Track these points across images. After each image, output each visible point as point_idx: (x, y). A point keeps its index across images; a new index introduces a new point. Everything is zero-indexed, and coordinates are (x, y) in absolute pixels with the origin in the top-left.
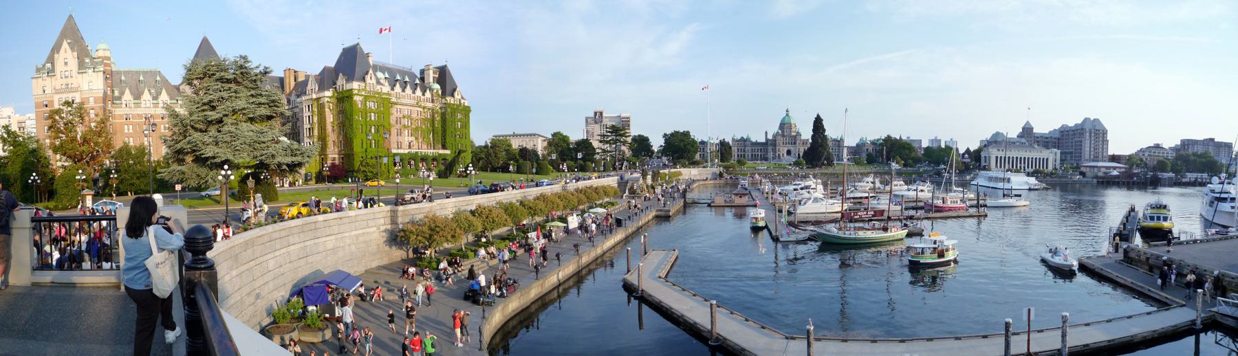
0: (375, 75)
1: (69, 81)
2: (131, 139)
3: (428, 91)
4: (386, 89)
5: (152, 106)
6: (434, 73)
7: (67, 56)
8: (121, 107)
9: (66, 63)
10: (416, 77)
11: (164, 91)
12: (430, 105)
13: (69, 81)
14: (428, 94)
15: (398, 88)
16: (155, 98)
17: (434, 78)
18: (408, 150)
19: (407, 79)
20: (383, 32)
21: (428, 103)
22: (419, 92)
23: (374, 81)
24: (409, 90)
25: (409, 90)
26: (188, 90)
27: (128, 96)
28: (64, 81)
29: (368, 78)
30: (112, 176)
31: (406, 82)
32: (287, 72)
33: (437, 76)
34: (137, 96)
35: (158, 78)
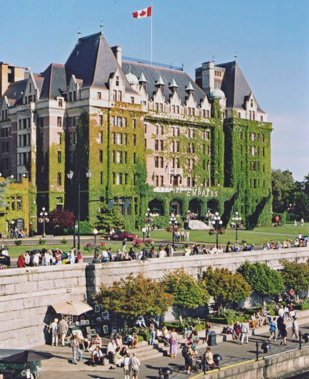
0: (125, 79)
3: (206, 100)
4: (141, 96)
6: (217, 73)
10: (189, 79)
15: (159, 98)
17: (216, 80)
18: (171, 189)
19: (174, 84)
20: (146, 10)
21: (206, 120)
22: (191, 103)
23: (121, 87)
24: (176, 100)
25: (176, 100)
29: (113, 82)
31: (172, 89)
33: (221, 78)
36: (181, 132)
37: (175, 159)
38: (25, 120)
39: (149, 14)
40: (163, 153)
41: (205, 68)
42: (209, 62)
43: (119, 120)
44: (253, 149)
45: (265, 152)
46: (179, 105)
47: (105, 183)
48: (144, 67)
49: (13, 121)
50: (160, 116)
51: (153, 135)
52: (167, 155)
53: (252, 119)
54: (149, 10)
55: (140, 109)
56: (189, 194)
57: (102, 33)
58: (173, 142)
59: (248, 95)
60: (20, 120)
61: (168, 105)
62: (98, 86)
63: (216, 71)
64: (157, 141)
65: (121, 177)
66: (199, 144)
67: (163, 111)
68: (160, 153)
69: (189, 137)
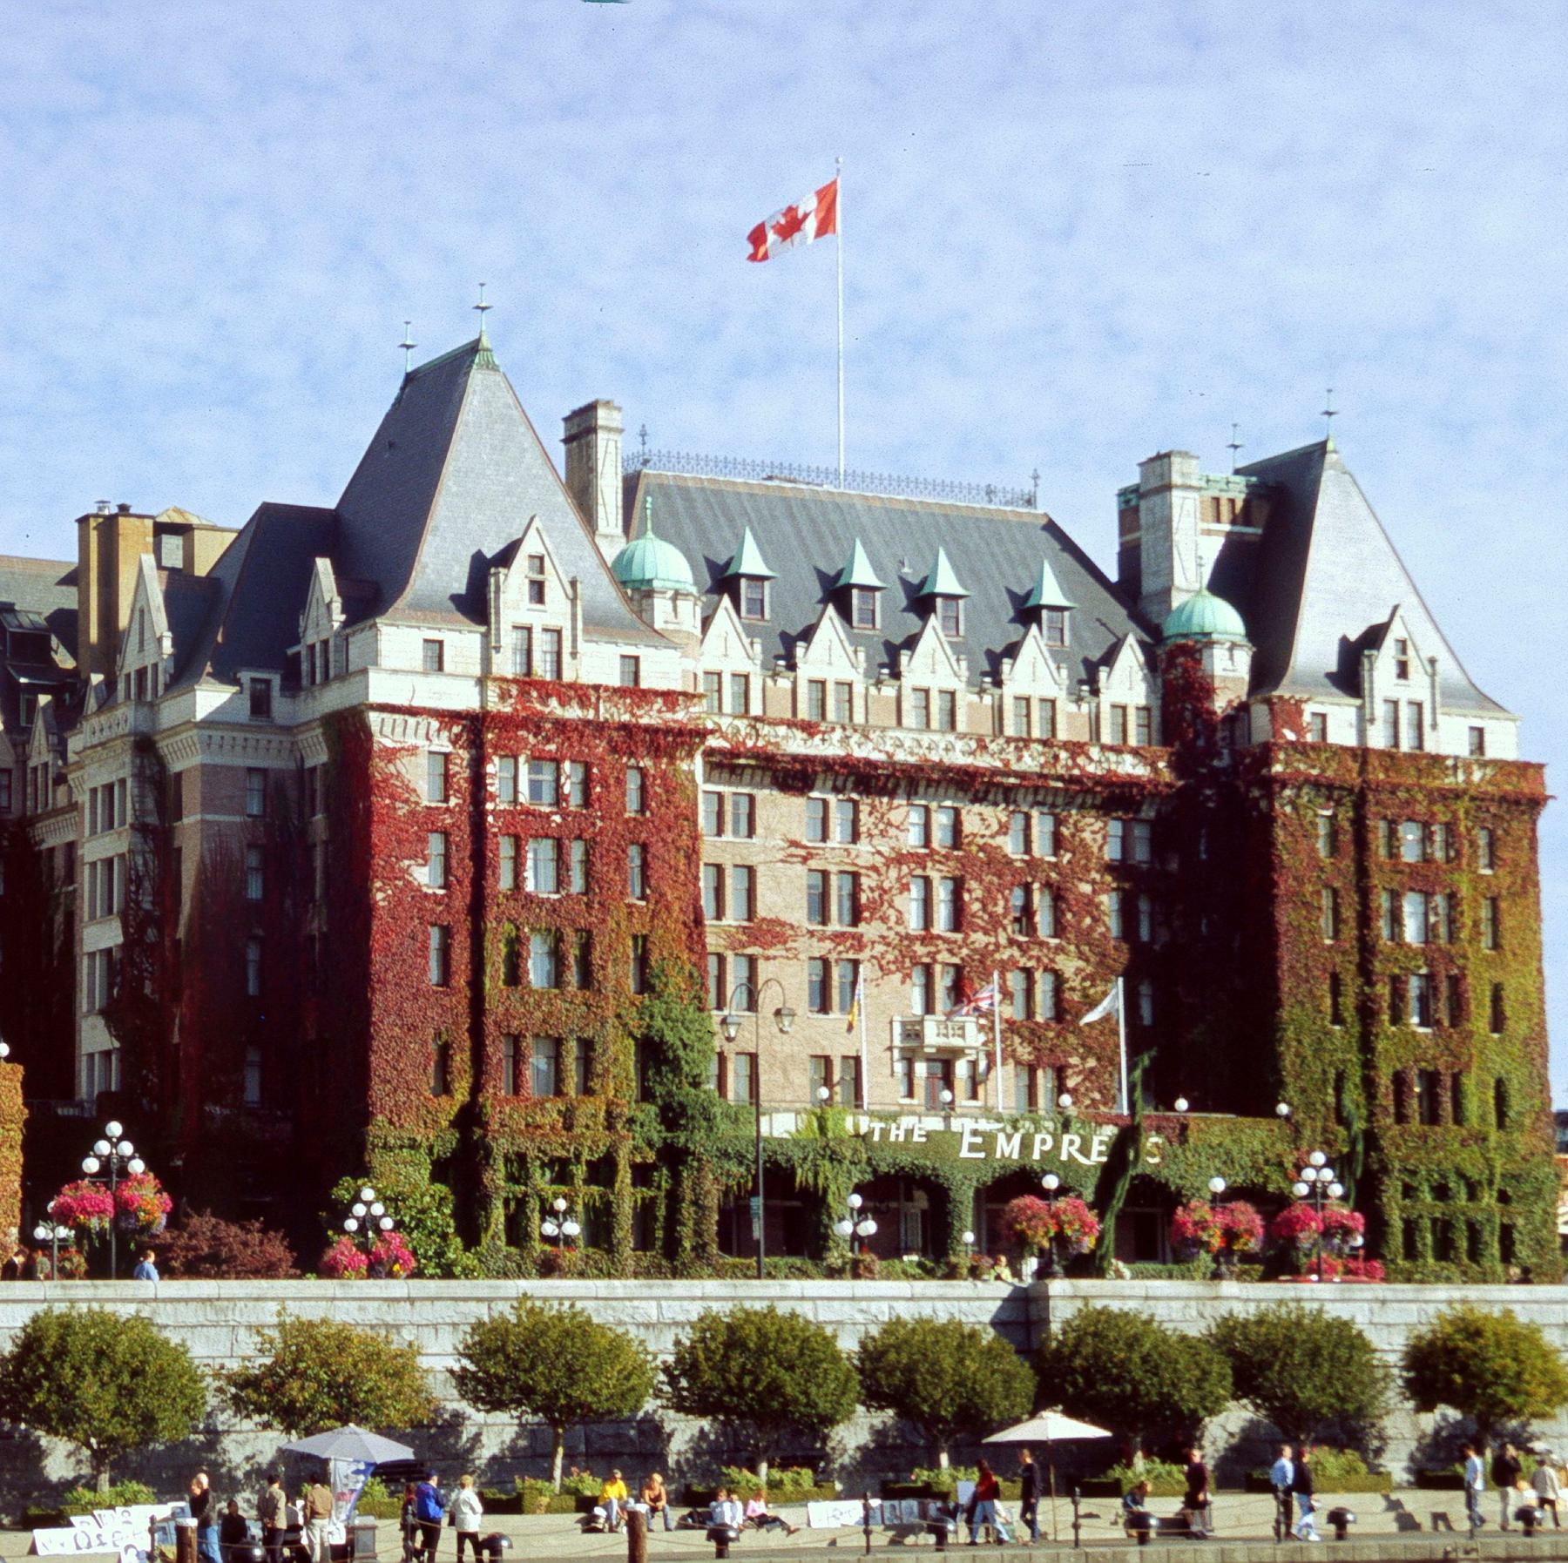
3: (1131, 657)
36: (971, 824)
37: (938, 968)
38: (109, 788)
39: (825, 225)
40: (859, 938)
41: (1154, 483)
42: (1168, 455)
43: (547, 776)
44: (1411, 907)
45: (1508, 922)
46: (959, 685)
47: (461, 1093)
48: (784, 499)
50: (829, 747)
51: (795, 844)
52: (880, 948)
53: (1406, 745)
54: (827, 197)
55: (669, 716)
56: (973, 1147)
57: (485, 342)
58: (927, 882)
59: (1383, 619)
60: (94, 791)
61: (889, 691)
62: (424, 610)
63: (1217, 500)
64: (825, 875)
65: (557, 1059)
66: (1086, 888)
67: (859, 718)
68: (838, 938)
69: (1028, 848)
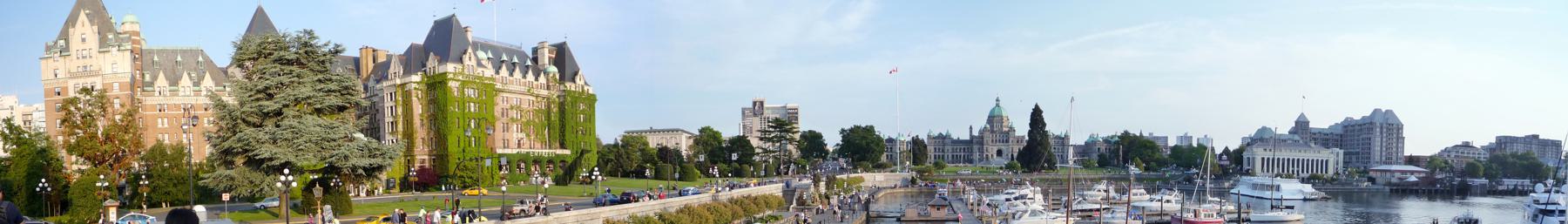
0: (475, 55)
1: (87, 62)
2: (166, 136)
3: (542, 75)
4: (489, 72)
5: (192, 94)
6: (550, 52)
7: (85, 30)
8: (153, 95)
9: (84, 40)
10: (528, 57)
11: (208, 76)
12: (545, 92)
13: (87, 62)
14: (542, 79)
15: (504, 72)
16: (197, 84)
17: (550, 58)
18: (518, 150)
19: (515, 60)
21: (542, 91)
22: (530, 77)
23: (474, 62)
24: (518, 74)
25: (518, 74)
26: (238, 74)
27: (162, 81)
28: (81, 62)
29: (466, 58)
30: (141, 183)
31: (514, 64)
32: (364, 51)
33: (554, 56)
34: (174, 81)
35: (200, 59)
49: (380, 95)
